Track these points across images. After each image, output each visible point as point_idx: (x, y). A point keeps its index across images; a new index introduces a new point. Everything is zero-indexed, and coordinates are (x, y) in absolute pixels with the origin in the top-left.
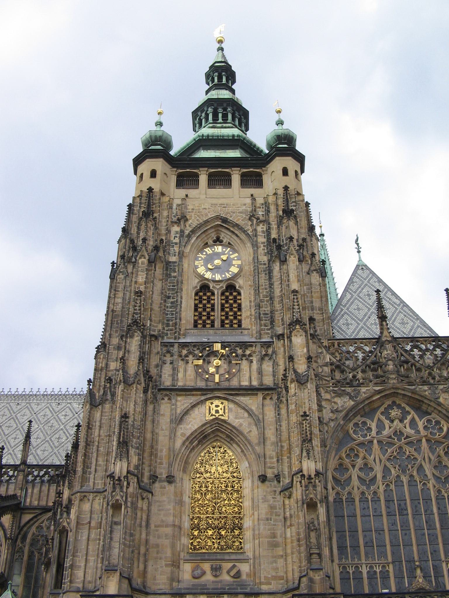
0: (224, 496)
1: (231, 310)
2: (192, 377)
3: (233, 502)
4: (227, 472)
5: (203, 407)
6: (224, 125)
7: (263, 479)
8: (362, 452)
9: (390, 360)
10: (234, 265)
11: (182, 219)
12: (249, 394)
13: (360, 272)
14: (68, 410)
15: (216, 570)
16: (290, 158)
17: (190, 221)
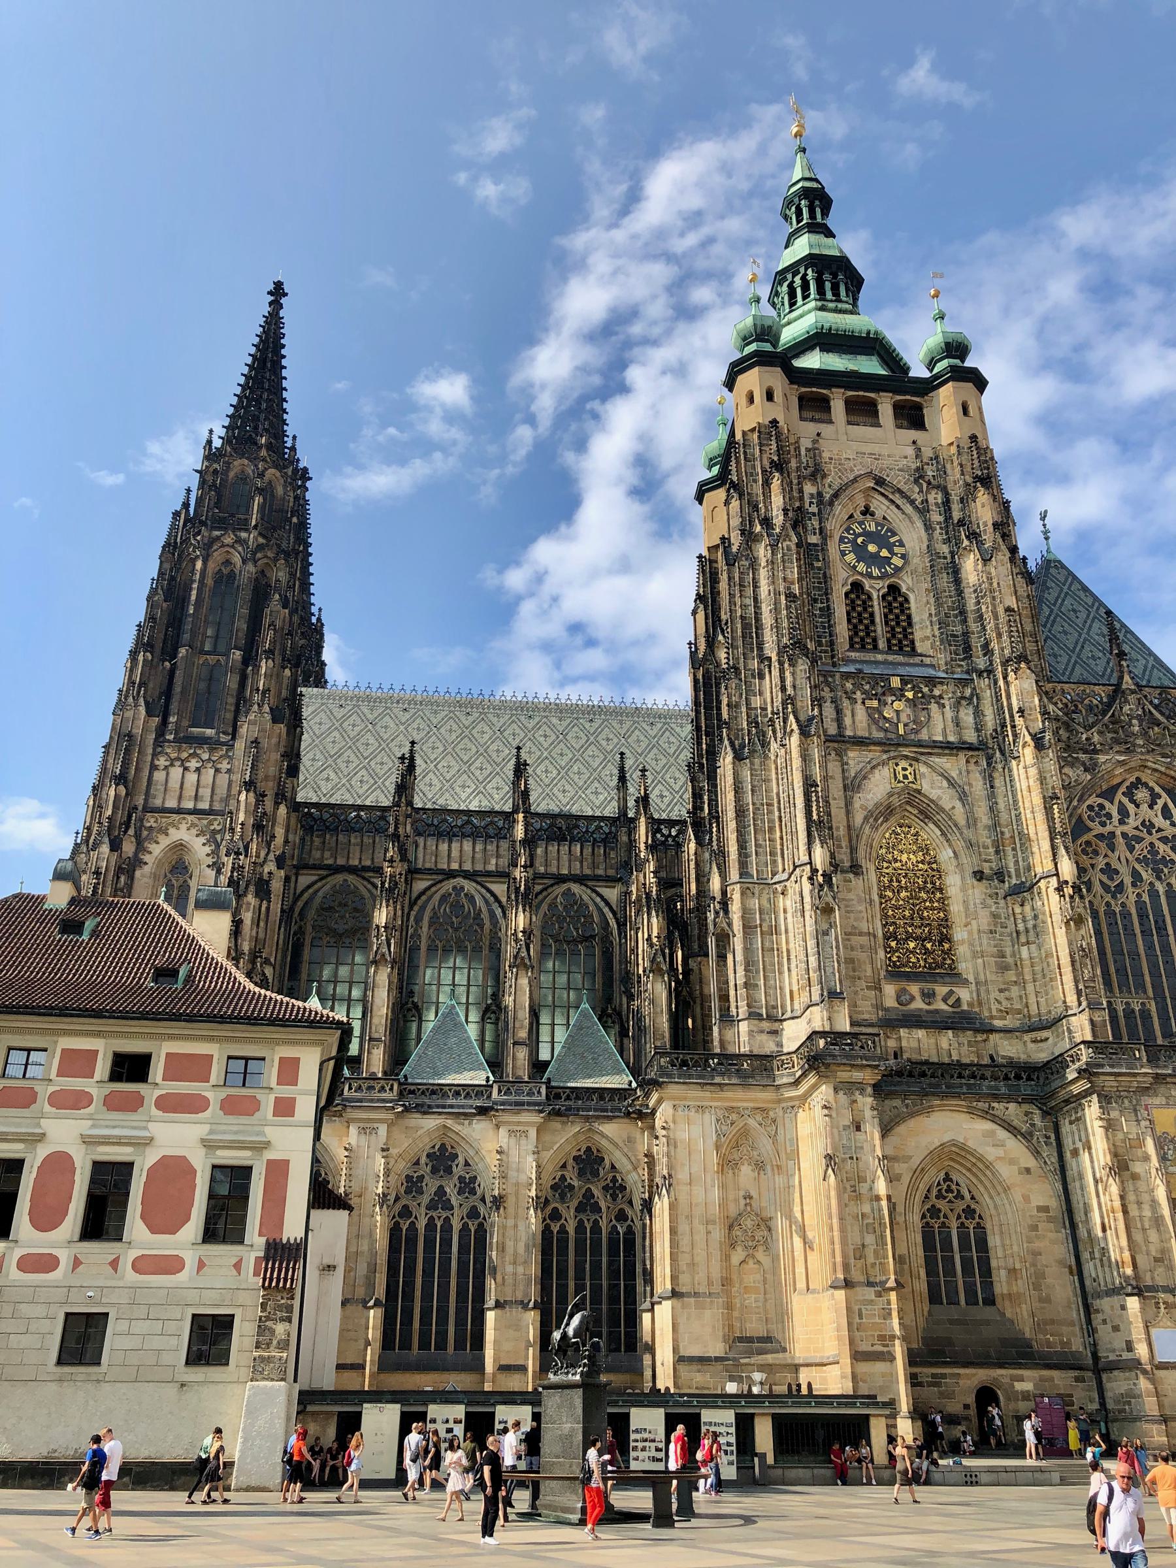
0: (923, 895)
1: (898, 624)
2: (865, 724)
3: (936, 904)
4: (922, 862)
5: (886, 769)
6: (840, 305)
7: (979, 875)
8: (1103, 847)
9: (1136, 718)
10: (896, 554)
11: (817, 473)
12: (946, 755)
13: (1053, 571)
14: (545, 727)
15: (928, 996)
16: (971, 385)
17: (829, 479)
